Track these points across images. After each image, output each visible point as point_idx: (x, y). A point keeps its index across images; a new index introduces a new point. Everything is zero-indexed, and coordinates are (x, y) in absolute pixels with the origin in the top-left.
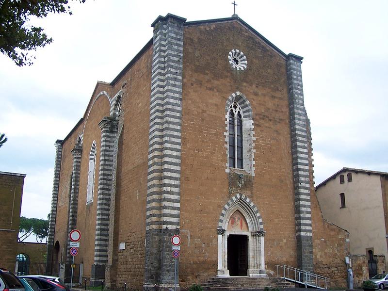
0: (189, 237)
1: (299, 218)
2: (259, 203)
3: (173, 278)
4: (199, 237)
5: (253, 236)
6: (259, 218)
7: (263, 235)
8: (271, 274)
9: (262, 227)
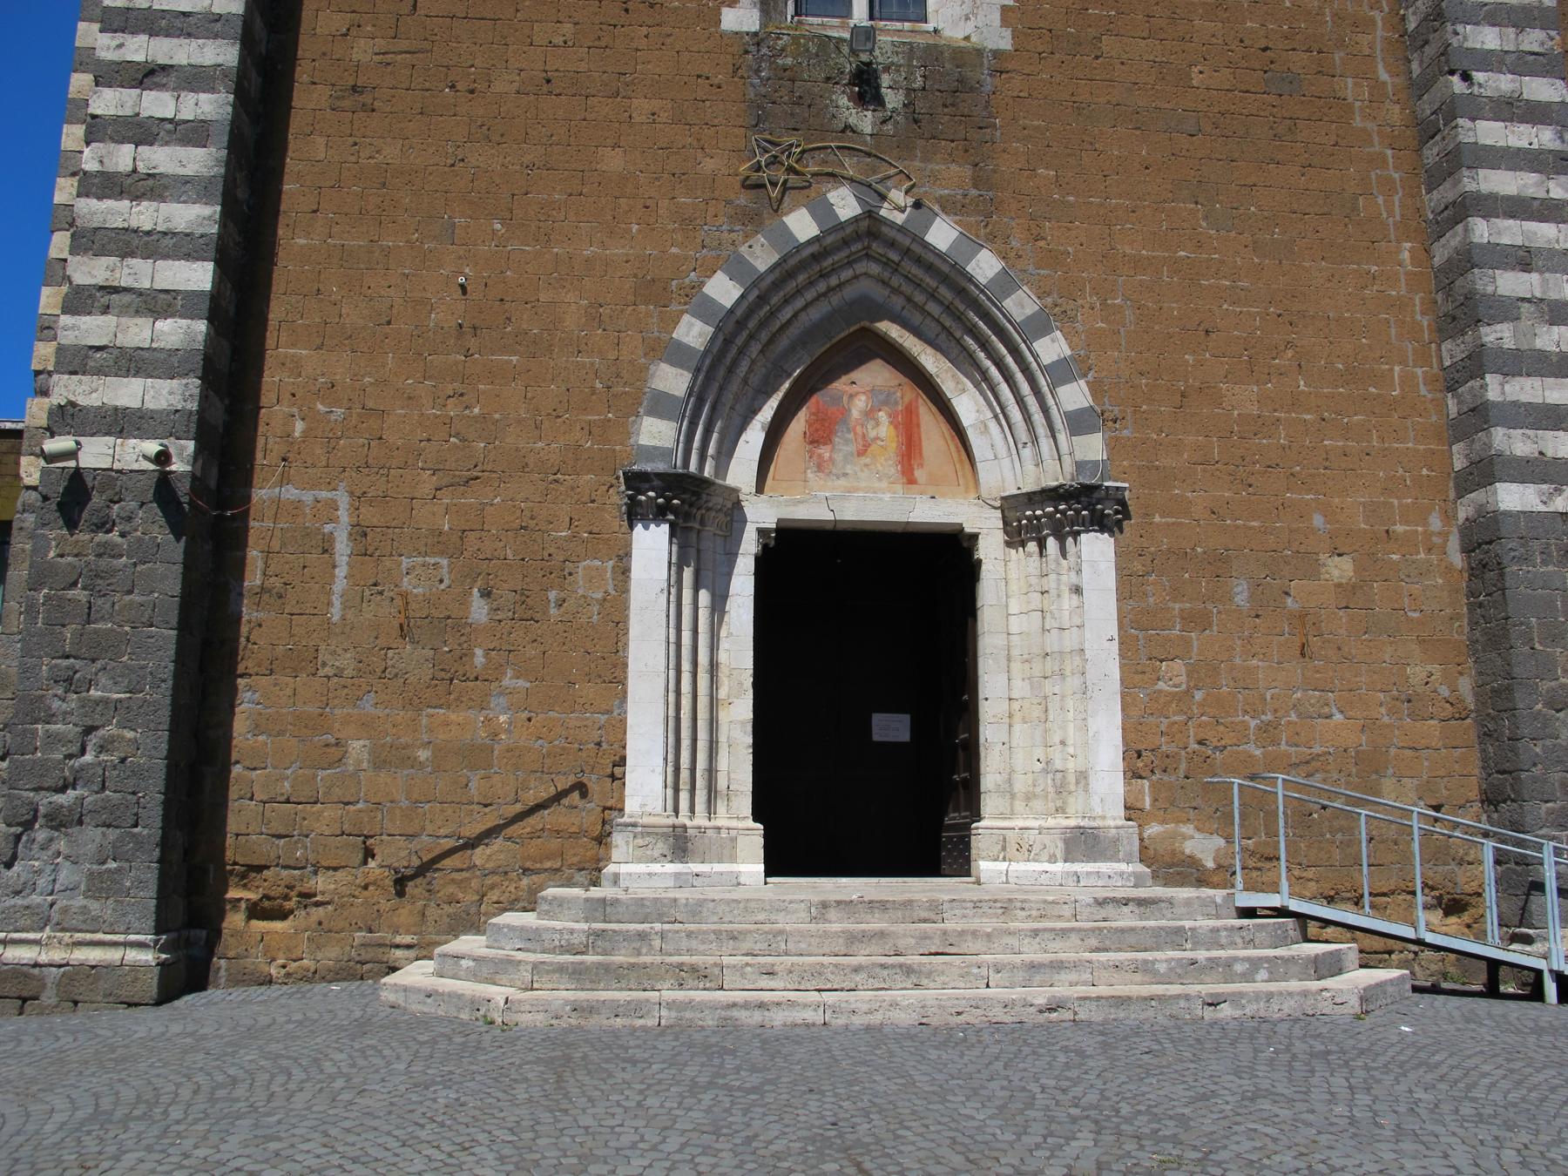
0: (342, 547)
1: (1477, 363)
2: (1053, 259)
3: (99, 886)
4: (439, 543)
5: (1015, 536)
6: (1061, 372)
7: (1101, 524)
8: (1193, 862)
9: (1093, 447)
